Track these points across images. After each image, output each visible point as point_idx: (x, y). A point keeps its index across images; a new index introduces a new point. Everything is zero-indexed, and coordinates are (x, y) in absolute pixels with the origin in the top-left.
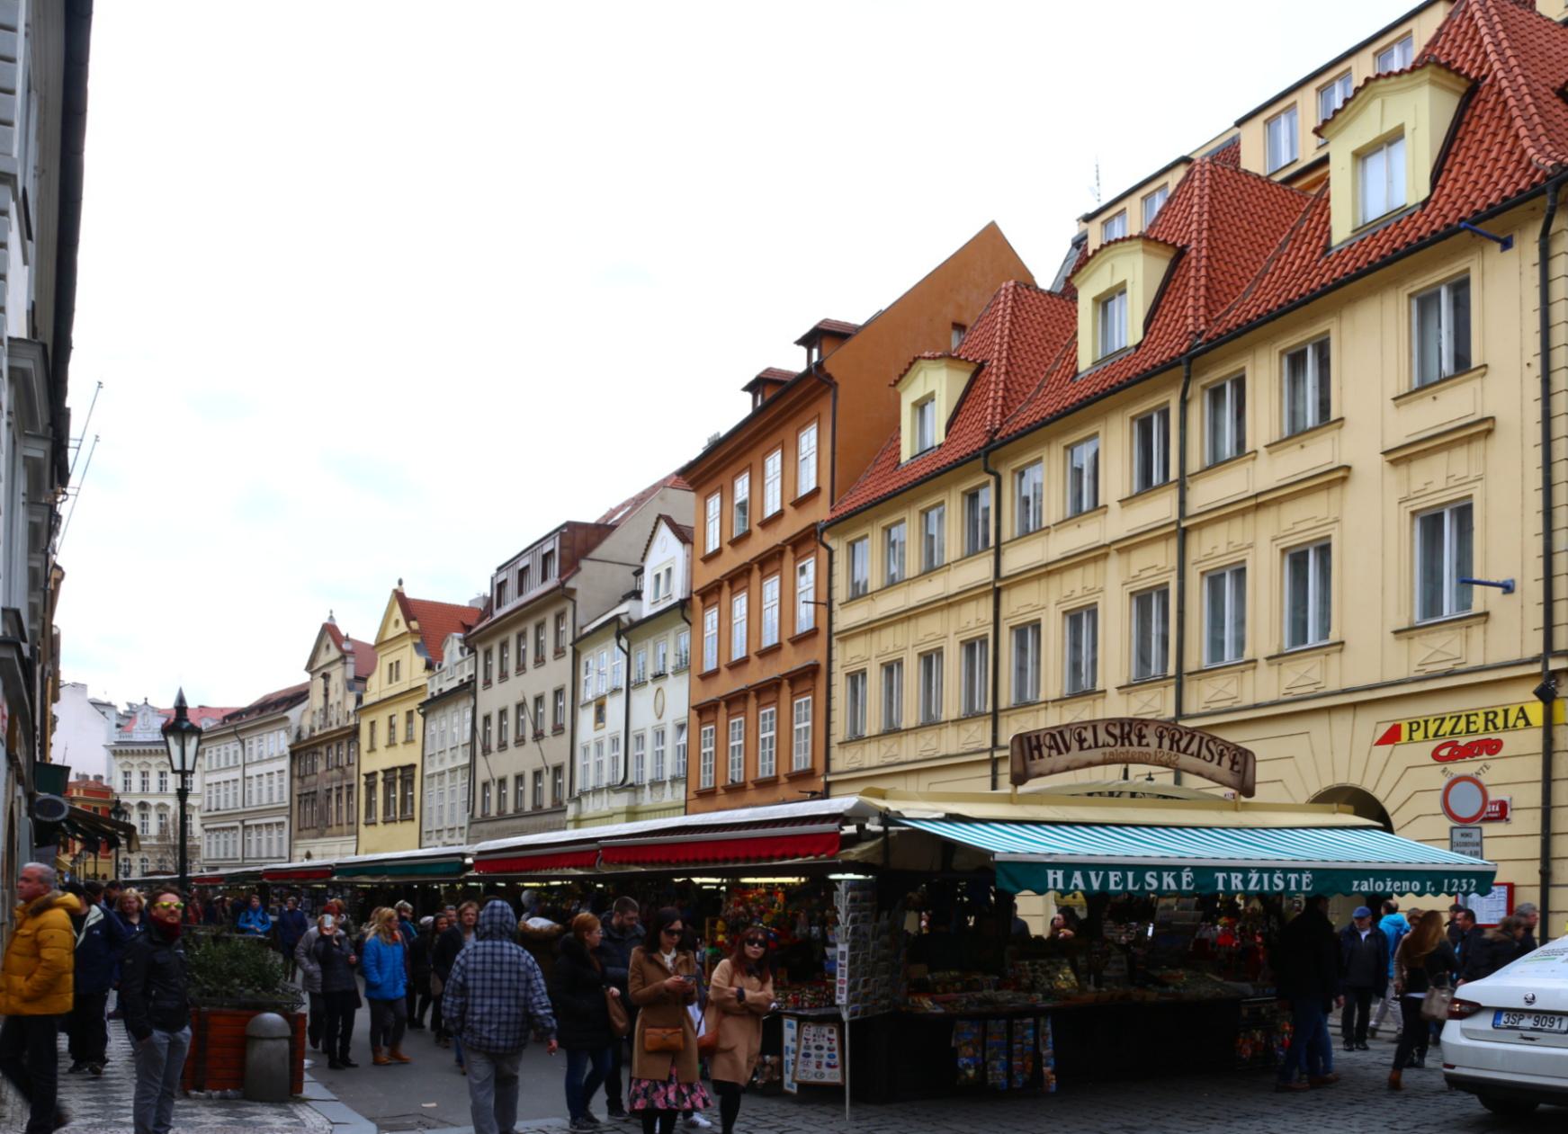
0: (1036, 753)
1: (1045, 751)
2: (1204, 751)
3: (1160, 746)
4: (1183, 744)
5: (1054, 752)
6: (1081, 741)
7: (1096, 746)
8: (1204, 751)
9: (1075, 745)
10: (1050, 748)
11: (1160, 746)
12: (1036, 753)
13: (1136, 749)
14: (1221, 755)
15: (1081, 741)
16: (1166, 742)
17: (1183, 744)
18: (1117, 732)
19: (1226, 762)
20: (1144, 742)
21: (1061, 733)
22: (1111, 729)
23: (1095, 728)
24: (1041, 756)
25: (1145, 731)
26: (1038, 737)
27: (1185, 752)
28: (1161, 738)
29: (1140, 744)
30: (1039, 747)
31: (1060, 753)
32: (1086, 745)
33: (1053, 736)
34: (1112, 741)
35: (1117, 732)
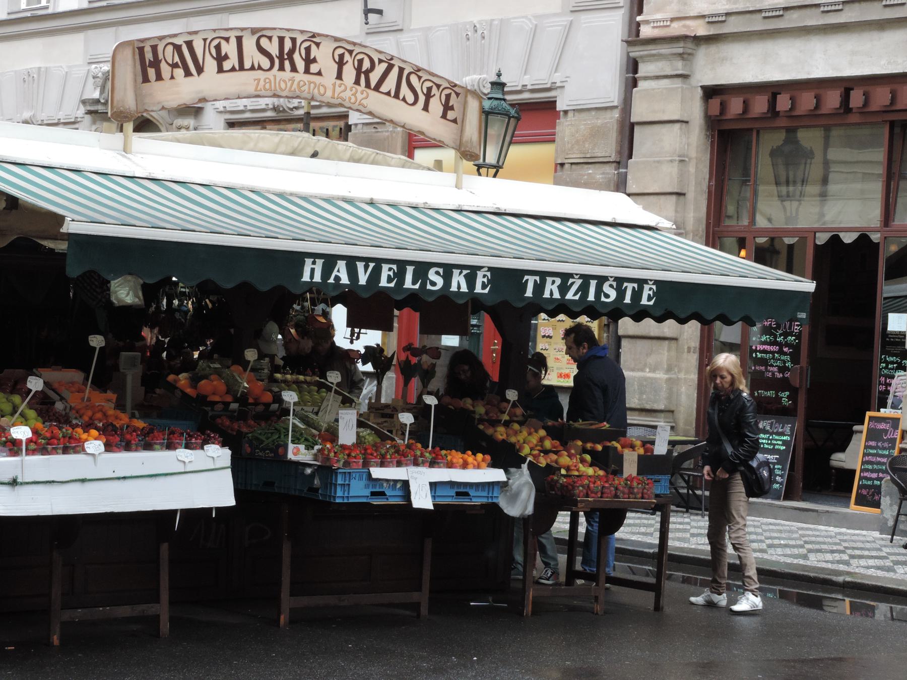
0: (151, 72)
1: (165, 69)
2: (405, 90)
3: (339, 76)
4: (374, 77)
5: (179, 72)
6: (220, 59)
7: (242, 68)
8: (405, 90)
9: (210, 65)
10: (174, 66)
11: (339, 76)
12: (151, 72)
13: (300, 76)
14: (428, 96)
15: (220, 59)
16: (349, 72)
17: (374, 77)
18: (274, 50)
19: (436, 105)
20: (314, 68)
21: (189, 44)
22: (264, 42)
23: (239, 40)
24: (159, 77)
25: (314, 52)
26: (154, 48)
27: (377, 88)
28: (341, 63)
29: (307, 71)
30: (156, 64)
31: (188, 73)
32: (227, 65)
33: (178, 48)
34: (266, 63)
35: (274, 50)
